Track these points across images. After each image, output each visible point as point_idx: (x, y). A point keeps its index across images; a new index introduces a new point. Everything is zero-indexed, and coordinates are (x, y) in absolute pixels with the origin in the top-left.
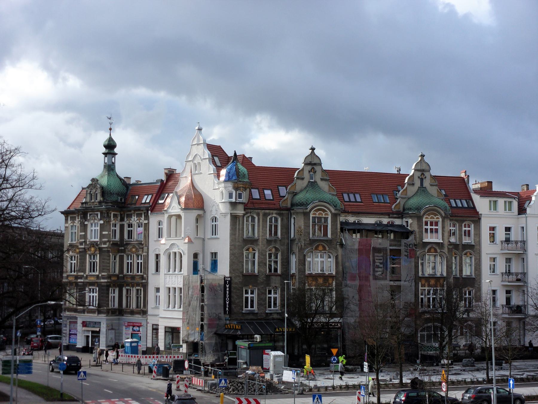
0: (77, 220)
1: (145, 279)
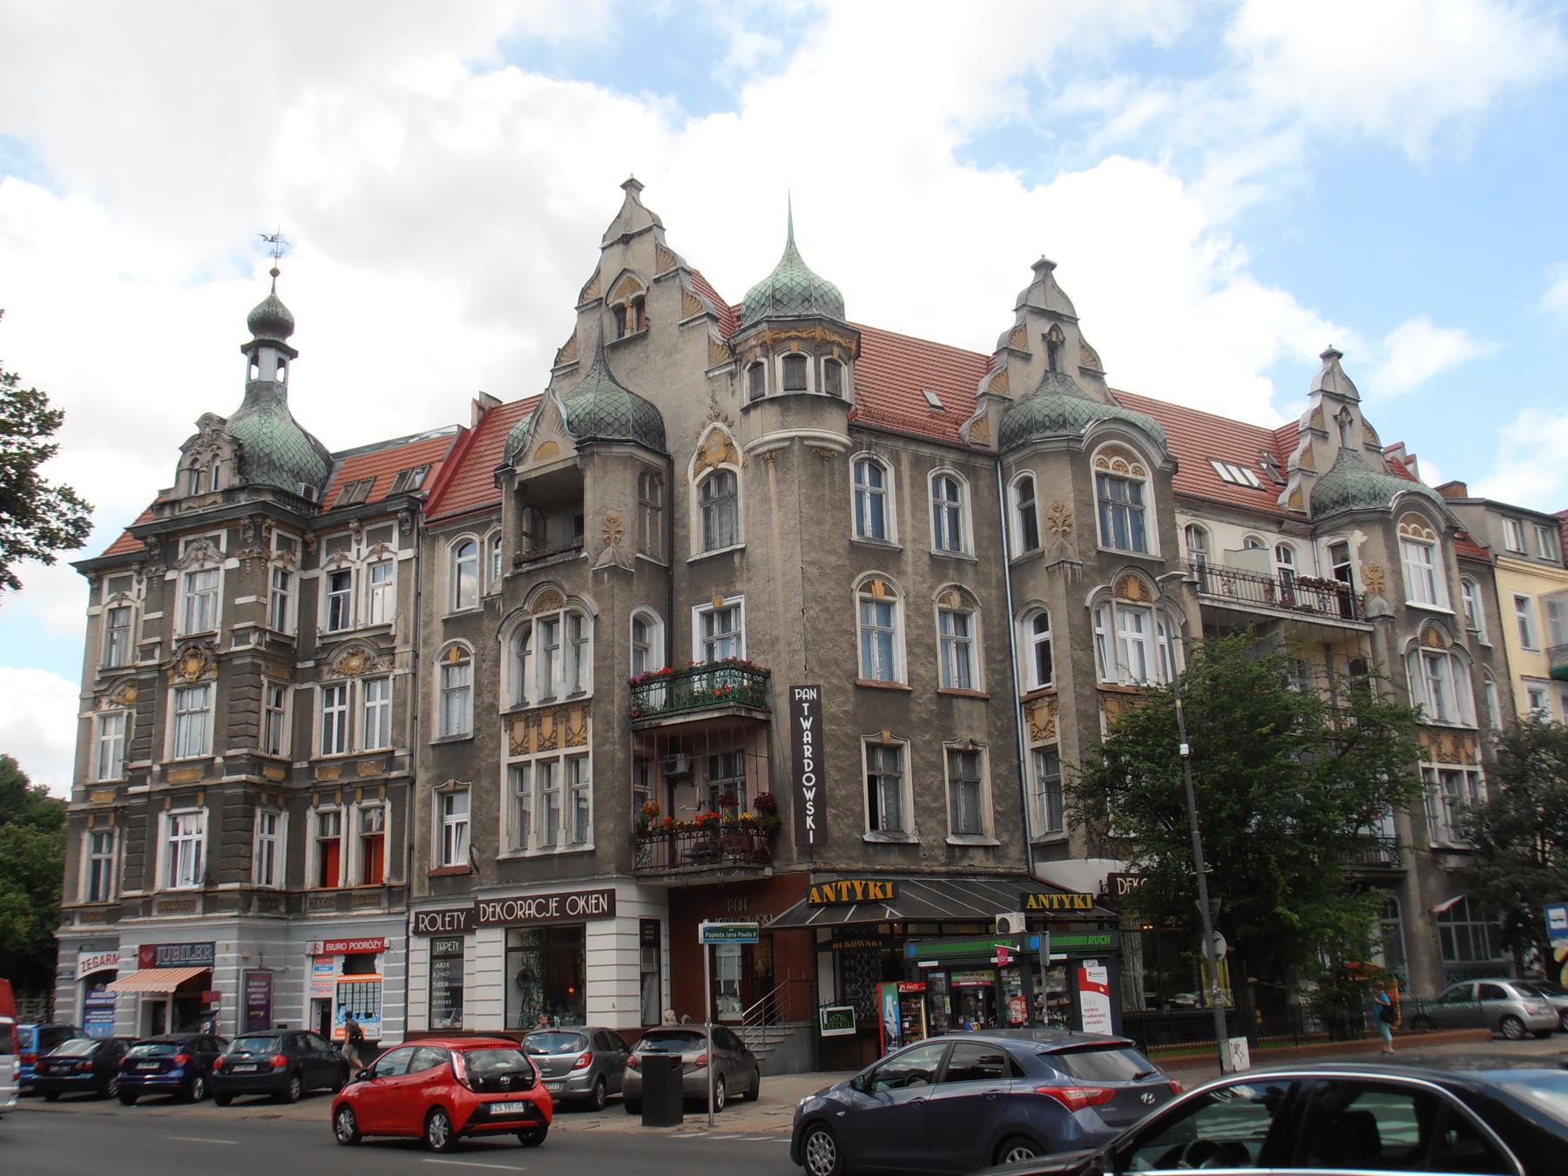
0: (135, 586)
1: (402, 767)
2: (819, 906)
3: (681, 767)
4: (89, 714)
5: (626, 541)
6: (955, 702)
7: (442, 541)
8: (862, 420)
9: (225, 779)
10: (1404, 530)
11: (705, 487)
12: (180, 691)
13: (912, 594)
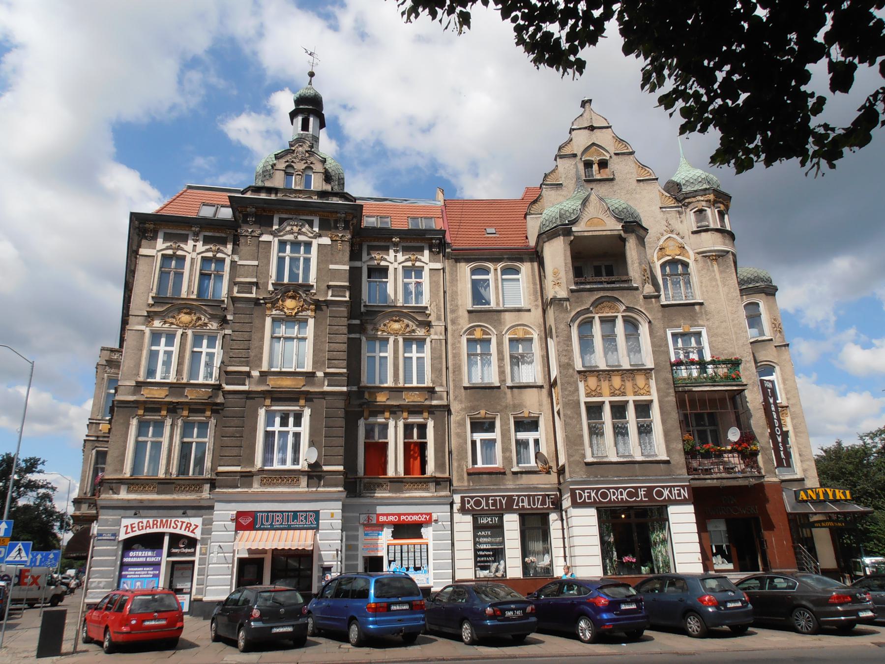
1: (441, 398)
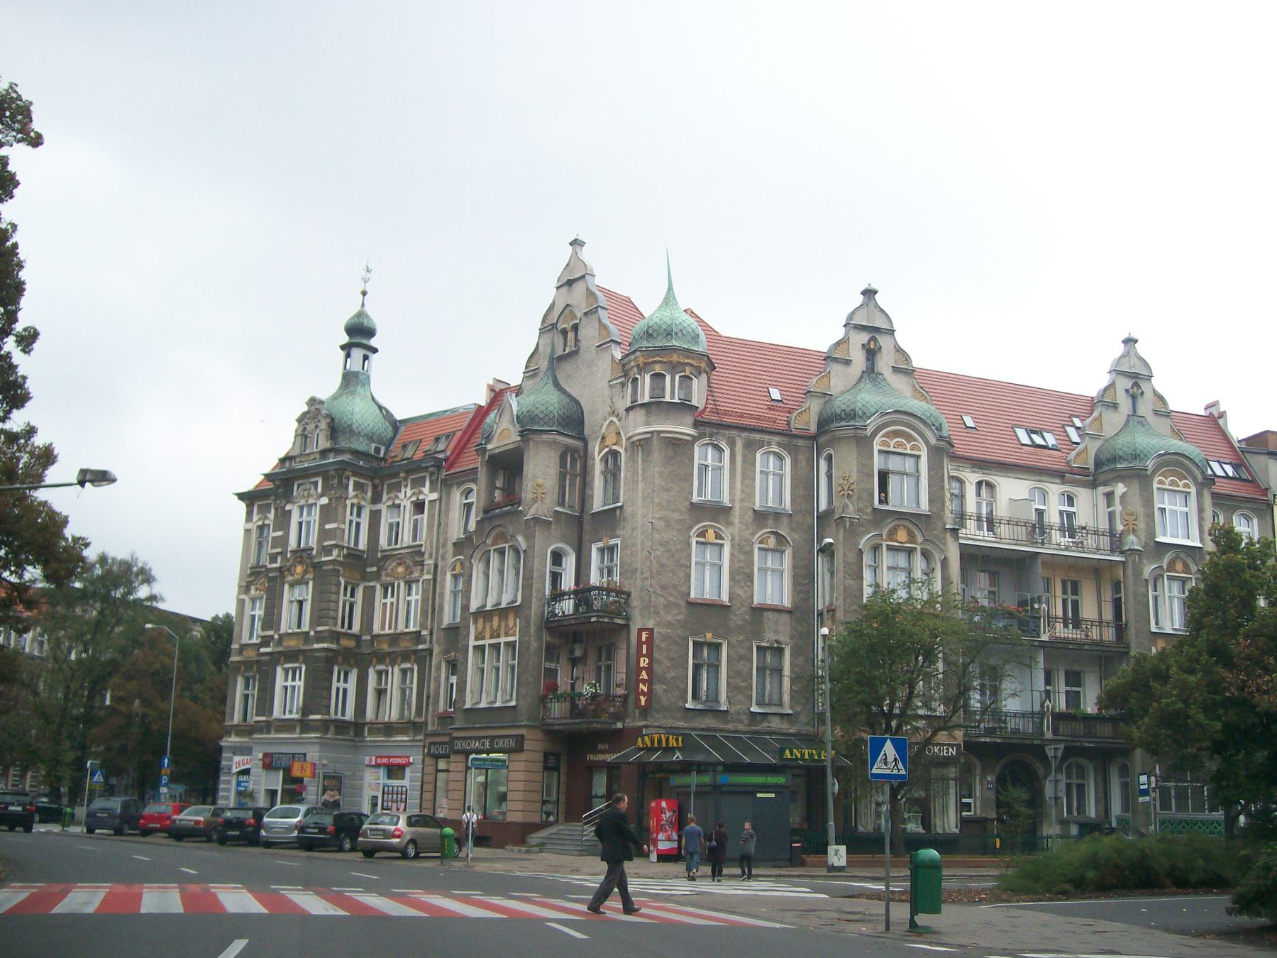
1: (424, 642)
2: (641, 749)
3: (578, 653)
4: (243, 596)
5: (548, 500)
6: (765, 613)
7: (455, 488)
8: (707, 417)
9: (316, 646)
10: (1160, 482)
11: (605, 460)
12: (292, 585)
13: (737, 538)
